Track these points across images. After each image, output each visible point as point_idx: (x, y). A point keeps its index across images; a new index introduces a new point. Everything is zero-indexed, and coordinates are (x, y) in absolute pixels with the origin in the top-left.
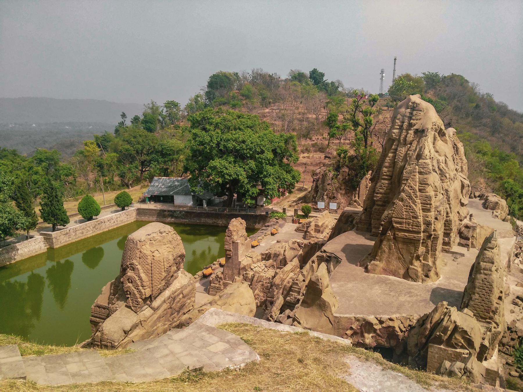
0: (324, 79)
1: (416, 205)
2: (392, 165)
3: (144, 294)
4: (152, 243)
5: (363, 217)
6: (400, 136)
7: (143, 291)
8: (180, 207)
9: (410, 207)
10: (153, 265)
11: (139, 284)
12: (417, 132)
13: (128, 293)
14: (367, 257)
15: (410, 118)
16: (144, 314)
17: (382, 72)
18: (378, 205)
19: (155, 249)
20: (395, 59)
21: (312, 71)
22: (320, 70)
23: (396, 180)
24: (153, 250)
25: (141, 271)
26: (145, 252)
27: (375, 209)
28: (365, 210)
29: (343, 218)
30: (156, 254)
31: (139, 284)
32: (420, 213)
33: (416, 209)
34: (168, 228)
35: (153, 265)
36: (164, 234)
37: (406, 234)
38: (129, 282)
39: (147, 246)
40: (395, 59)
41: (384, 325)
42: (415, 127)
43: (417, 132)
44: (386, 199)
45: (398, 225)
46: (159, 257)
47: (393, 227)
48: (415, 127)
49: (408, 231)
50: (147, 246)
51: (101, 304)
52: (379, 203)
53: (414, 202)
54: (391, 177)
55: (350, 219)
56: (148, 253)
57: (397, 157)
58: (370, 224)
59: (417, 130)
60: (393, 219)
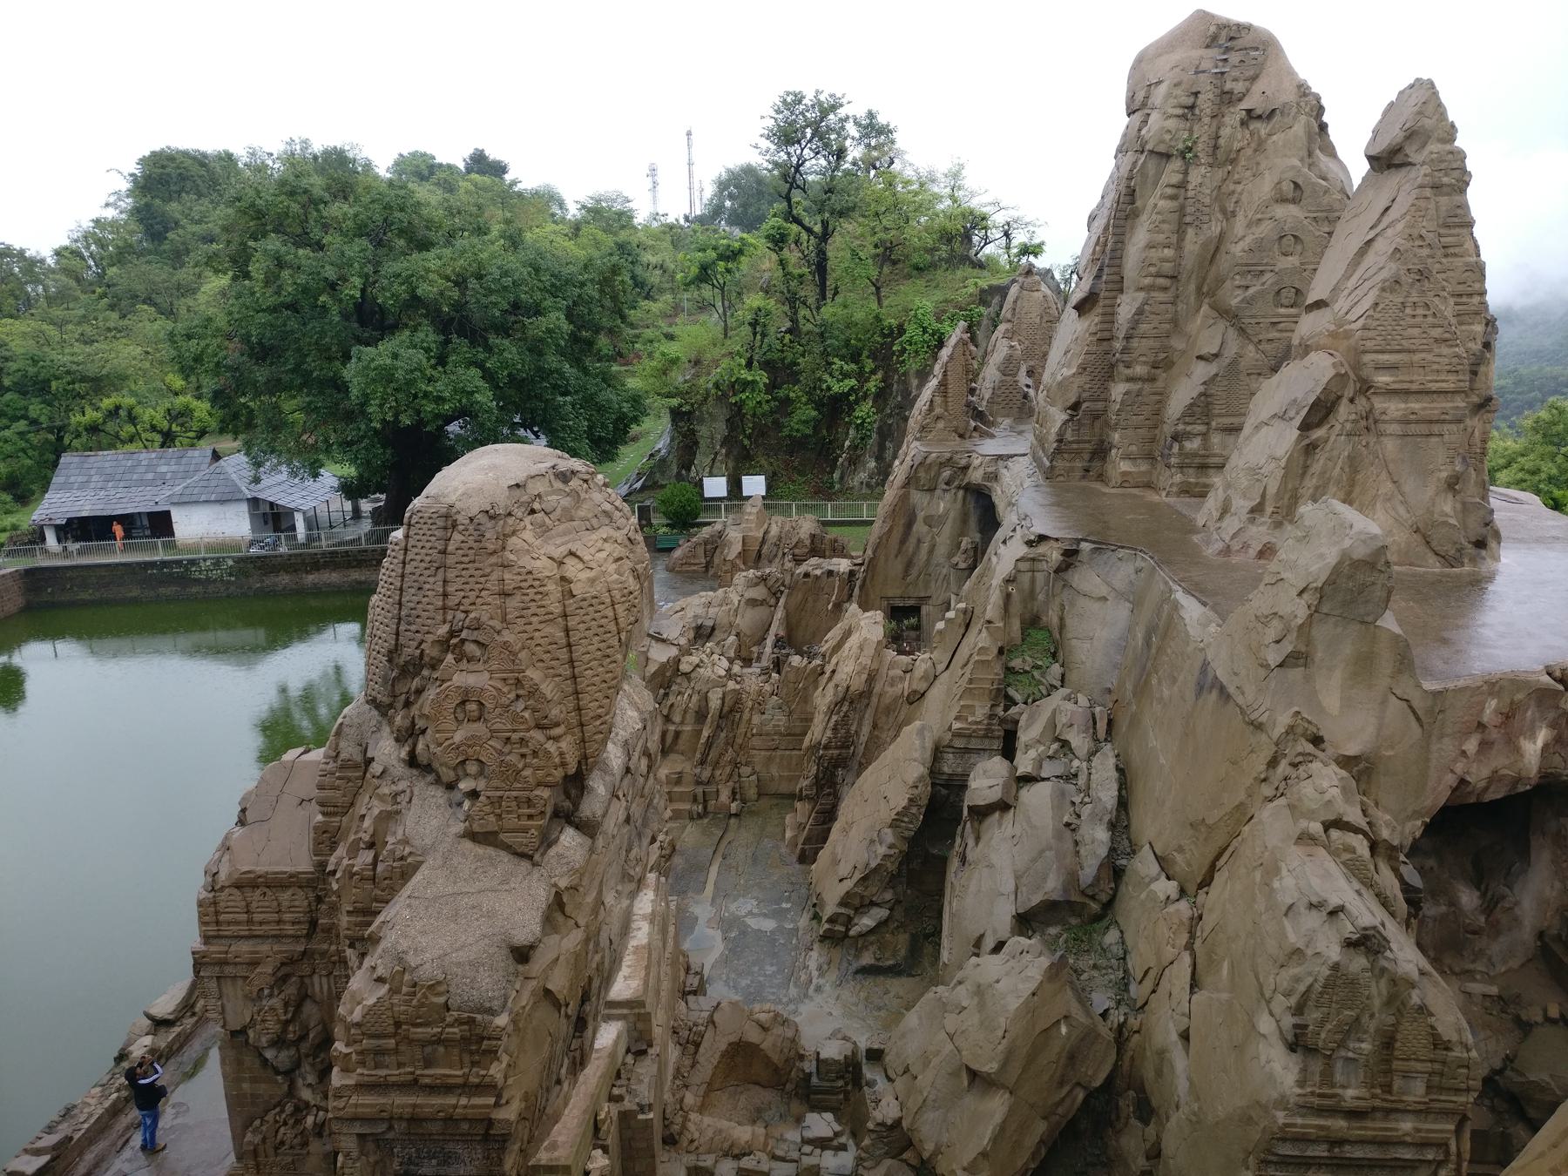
2: (1174, 238)
10: (572, 623)
13: (472, 768)
16: (560, 856)
17: (653, 171)
18: (1130, 379)
19: (563, 550)
20: (689, 134)
22: (493, 154)
24: (558, 553)
26: (527, 562)
29: (922, 474)
30: (572, 568)
35: (572, 623)
36: (575, 483)
37: (1416, 406)
39: (528, 535)
40: (689, 134)
42: (1245, 105)
44: (1162, 356)
46: (592, 581)
48: (1245, 105)
50: (528, 535)
51: (261, 869)
52: (1139, 370)
55: (947, 473)
56: (543, 566)
57: (1189, 210)
59: (1249, 111)
60: (1367, 358)
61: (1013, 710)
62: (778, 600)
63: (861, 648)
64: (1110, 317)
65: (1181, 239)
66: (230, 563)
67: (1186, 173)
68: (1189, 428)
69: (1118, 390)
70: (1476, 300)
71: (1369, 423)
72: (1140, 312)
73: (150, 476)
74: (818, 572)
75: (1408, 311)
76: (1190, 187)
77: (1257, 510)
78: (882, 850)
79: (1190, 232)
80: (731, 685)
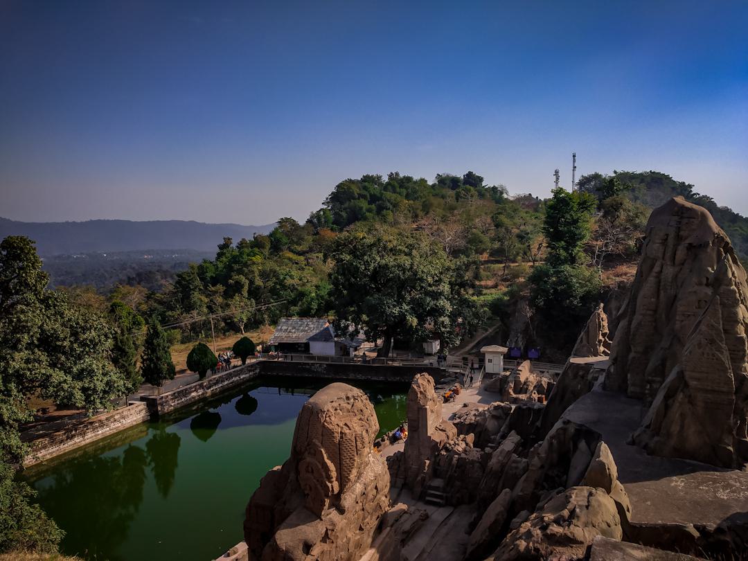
0: (484, 184)
1: (722, 353)
3: (331, 489)
4: (339, 414)
5: (612, 370)
6: (664, 254)
7: (329, 485)
8: (320, 358)
9: (713, 355)
11: (324, 474)
12: (690, 247)
13: (308, 488)
14: (645, 431)
15: (679, 229)
16: (330, 518)
17: (557, 173)
20: (574, 156)
21: (467, 175)
23: (663, 316)
25: (325, 456)
26: (330, 427)
27: (634, 358)
28: (615, 361)
30: (346, 430)
31: (324, 474)
32: (728, 363)
33: (723, 359)
34: (356, 391)
37: (709, 396)
38: (307, 471)
40: (574, 156)
41: (711, 540)
43: (690, 247)
45: (695, 383)
47: (686, 385)
48: (688, 241)
49: (713, 391)
53: (720, 349)
54: (655, 311)
55: (581, 373)
57: (662, 284)
58: (625, 380)
59: (690, 244)
61: (541, 492)
62: (507, 416)
63: (501, 452)
64: (630, 323)
65: (658, 296)
66: (325, 366)
67: (662, 268)
68: (654, 378)
69: (632, 355)
70: (741, 353)
71: (691, 401)
72: (639, 324)
73: (306, 329)
74: (525, 407)
75: (705, 356)
76: (663, 274)
77: (648, 427)
78: (484, 538)
79: (662, 292)
80: (463, 455)
